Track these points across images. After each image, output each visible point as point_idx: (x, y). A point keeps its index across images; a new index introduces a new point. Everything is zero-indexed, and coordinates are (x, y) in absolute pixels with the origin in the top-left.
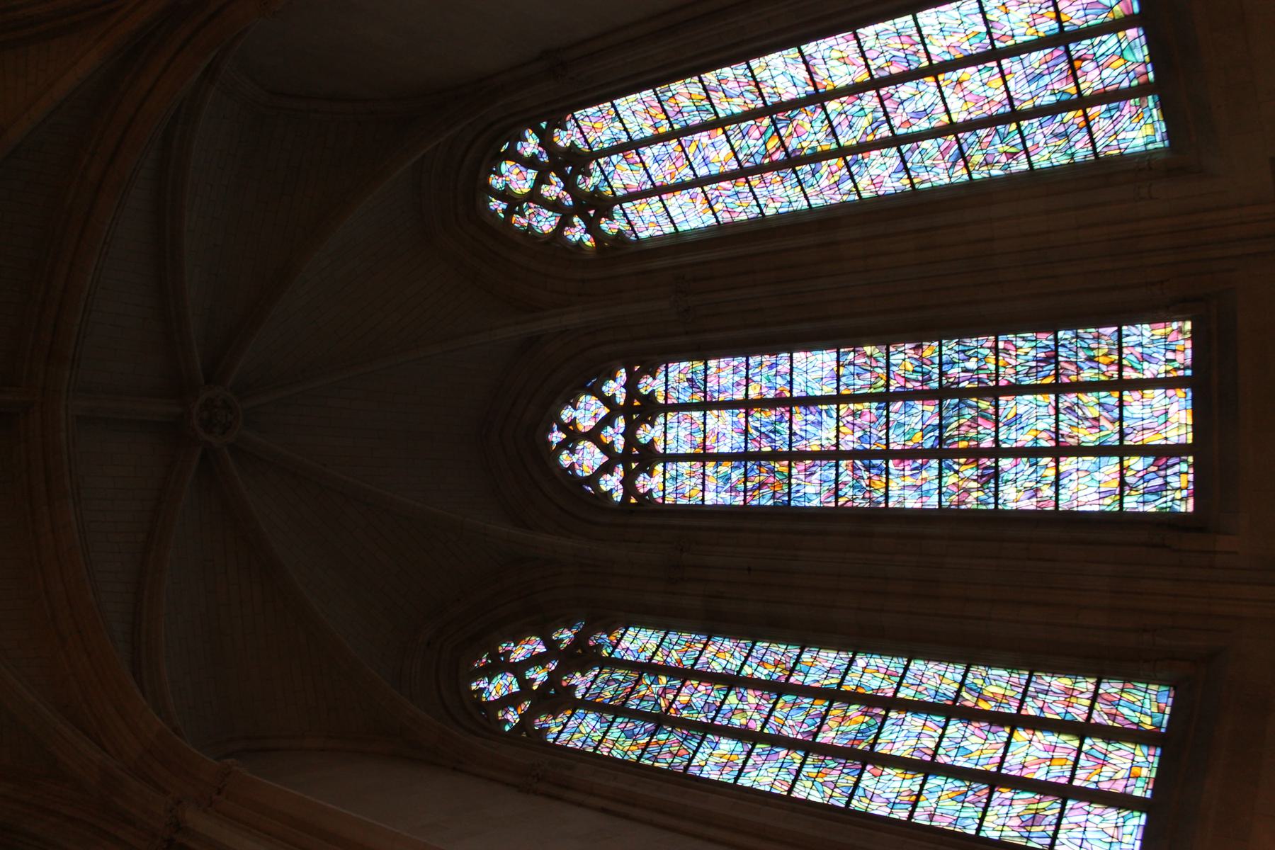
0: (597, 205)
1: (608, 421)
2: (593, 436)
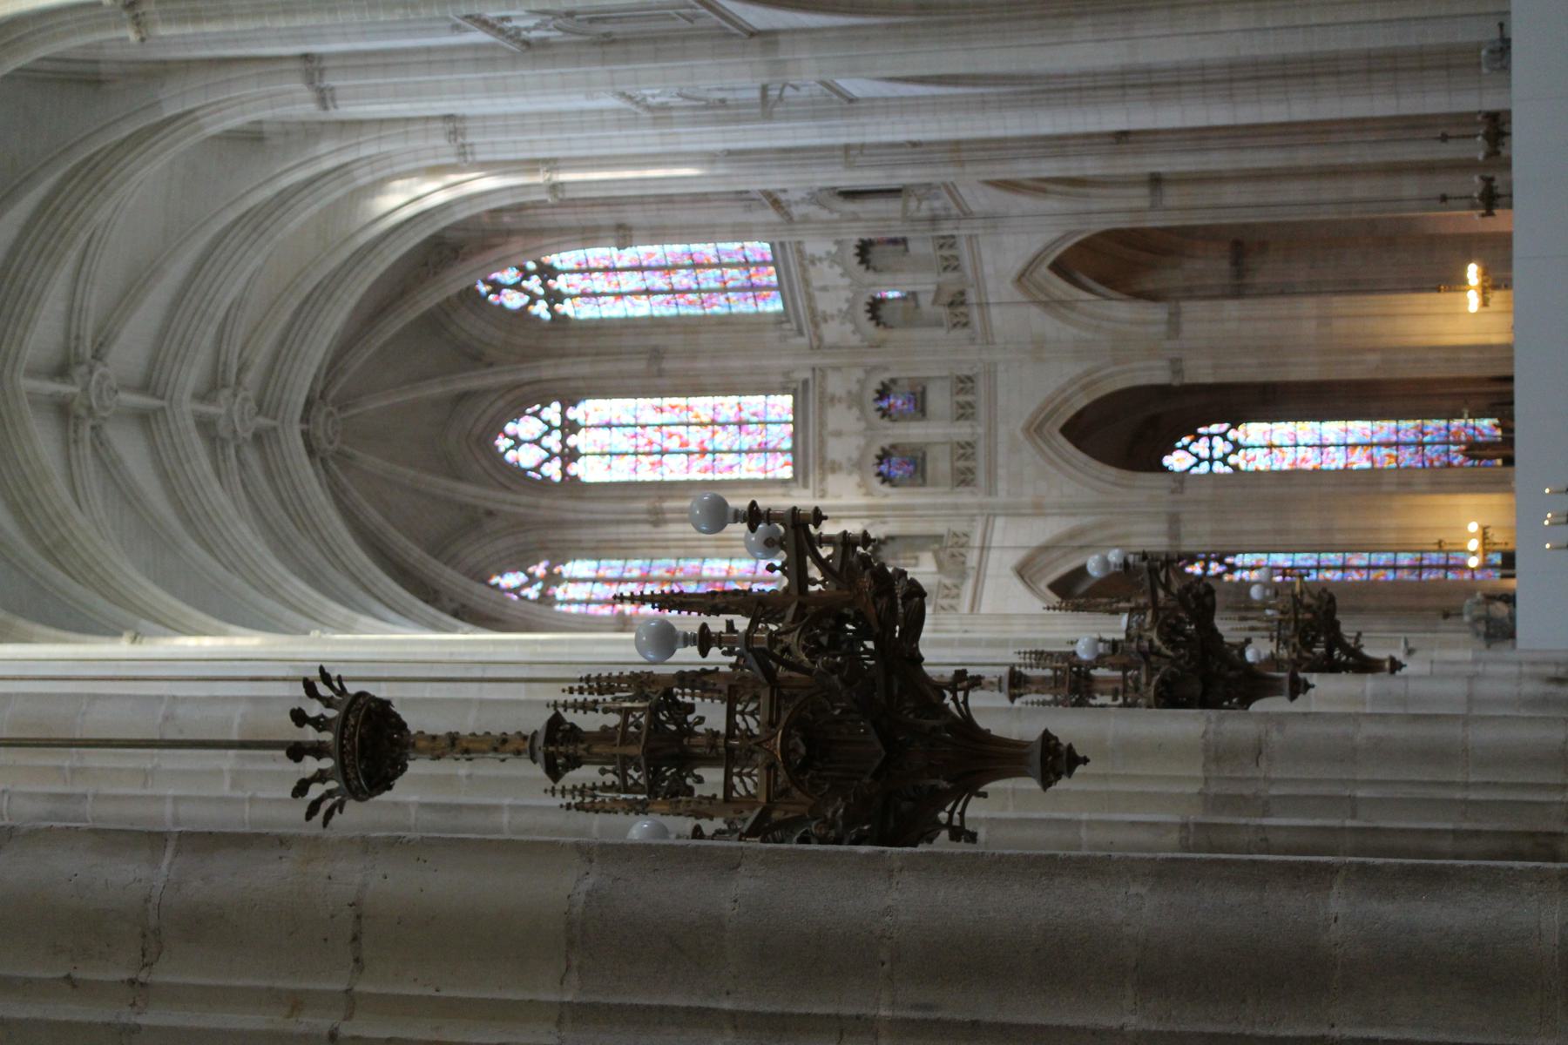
0: (554, 297)
1: (548, 433)
2: (537, 442)
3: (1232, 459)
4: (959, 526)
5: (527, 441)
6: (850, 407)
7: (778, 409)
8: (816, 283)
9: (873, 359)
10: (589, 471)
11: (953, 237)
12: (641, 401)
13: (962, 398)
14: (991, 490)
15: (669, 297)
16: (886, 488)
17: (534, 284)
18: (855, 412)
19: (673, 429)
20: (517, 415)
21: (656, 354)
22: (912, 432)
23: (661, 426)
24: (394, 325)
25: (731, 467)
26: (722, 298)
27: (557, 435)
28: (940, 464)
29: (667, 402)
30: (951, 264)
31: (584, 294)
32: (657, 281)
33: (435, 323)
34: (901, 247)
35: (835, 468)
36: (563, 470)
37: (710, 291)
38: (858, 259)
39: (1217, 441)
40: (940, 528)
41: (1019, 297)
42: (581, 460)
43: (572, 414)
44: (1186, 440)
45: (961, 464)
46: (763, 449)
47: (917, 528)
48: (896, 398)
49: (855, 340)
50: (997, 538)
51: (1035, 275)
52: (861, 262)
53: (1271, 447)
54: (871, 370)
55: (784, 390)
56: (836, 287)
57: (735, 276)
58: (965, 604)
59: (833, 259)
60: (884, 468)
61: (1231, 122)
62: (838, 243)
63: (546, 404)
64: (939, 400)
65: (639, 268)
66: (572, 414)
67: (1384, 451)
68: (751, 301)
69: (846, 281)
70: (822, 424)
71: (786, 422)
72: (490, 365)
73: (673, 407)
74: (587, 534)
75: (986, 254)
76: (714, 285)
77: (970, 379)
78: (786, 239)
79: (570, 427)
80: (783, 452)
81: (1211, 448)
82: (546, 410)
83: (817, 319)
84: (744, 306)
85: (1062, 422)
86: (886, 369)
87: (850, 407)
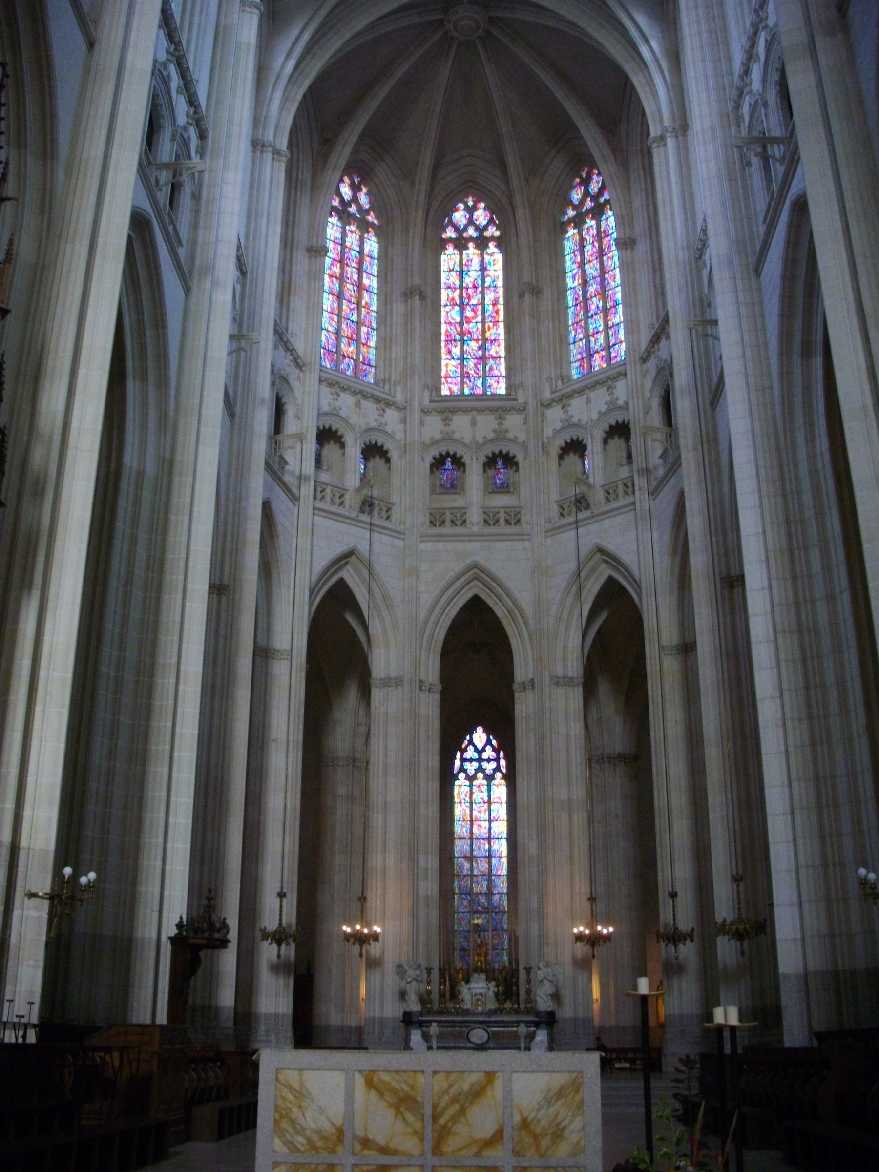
1: (477, 228)
2: (471, 222)
4: (395, 513)
6: (494, 431)
7: (495, 385)
8: (593, 395)
10: (449, 258)
11: (634, 493)
12: (501, 291)
13: (502, 516)
14: (425, 537)
15: (581, 299)
16: (429, 460)
17: (589, 204)
18: (491, 436)
19: (480, 313)
21: (536, 291)
22: (475, 477)
23: (483, 304)
25: (449, 352)
26: (581, 336)
27: (475, 235)
29: (501, 308)
31: (582, 240)
32: (592, 289)
34: (624, 462)
35: (447, 421)
36: (450, 240)
37: (586, 328)
38: (613, 423)
39: (493, 765)
41: (584, 552)
42: (456, 252)
43: (491, 245)
44: (494, 742)
46: (464, 376)
47: (396, 481)
48: (501, 461)
49: (548, 432)
51: (604, 565)
52: (611, 427)
53: (489, 802)
54: (524, 446)
57: (597, 323)
59: (613, 407)
60: (449, 465)
61: (753, 639)
62: (627, 403)
64: (501, 501)
65: (603, 271)
66: (492, 248)
67: (485, 884)
68: (579, 357)
69: (595, 416)
70: (481, 410)
71: (485, 391)
72: (527, 180)
73: (497, 312)
75: (619, 520)
76: (591, 327)
78: (628, 364)
79: (482, 243)
80: (462, 389)
81: (489, 760)
82: (495, 228)
84: (575, 352)
85: (483, 596)
87: (494, 431)
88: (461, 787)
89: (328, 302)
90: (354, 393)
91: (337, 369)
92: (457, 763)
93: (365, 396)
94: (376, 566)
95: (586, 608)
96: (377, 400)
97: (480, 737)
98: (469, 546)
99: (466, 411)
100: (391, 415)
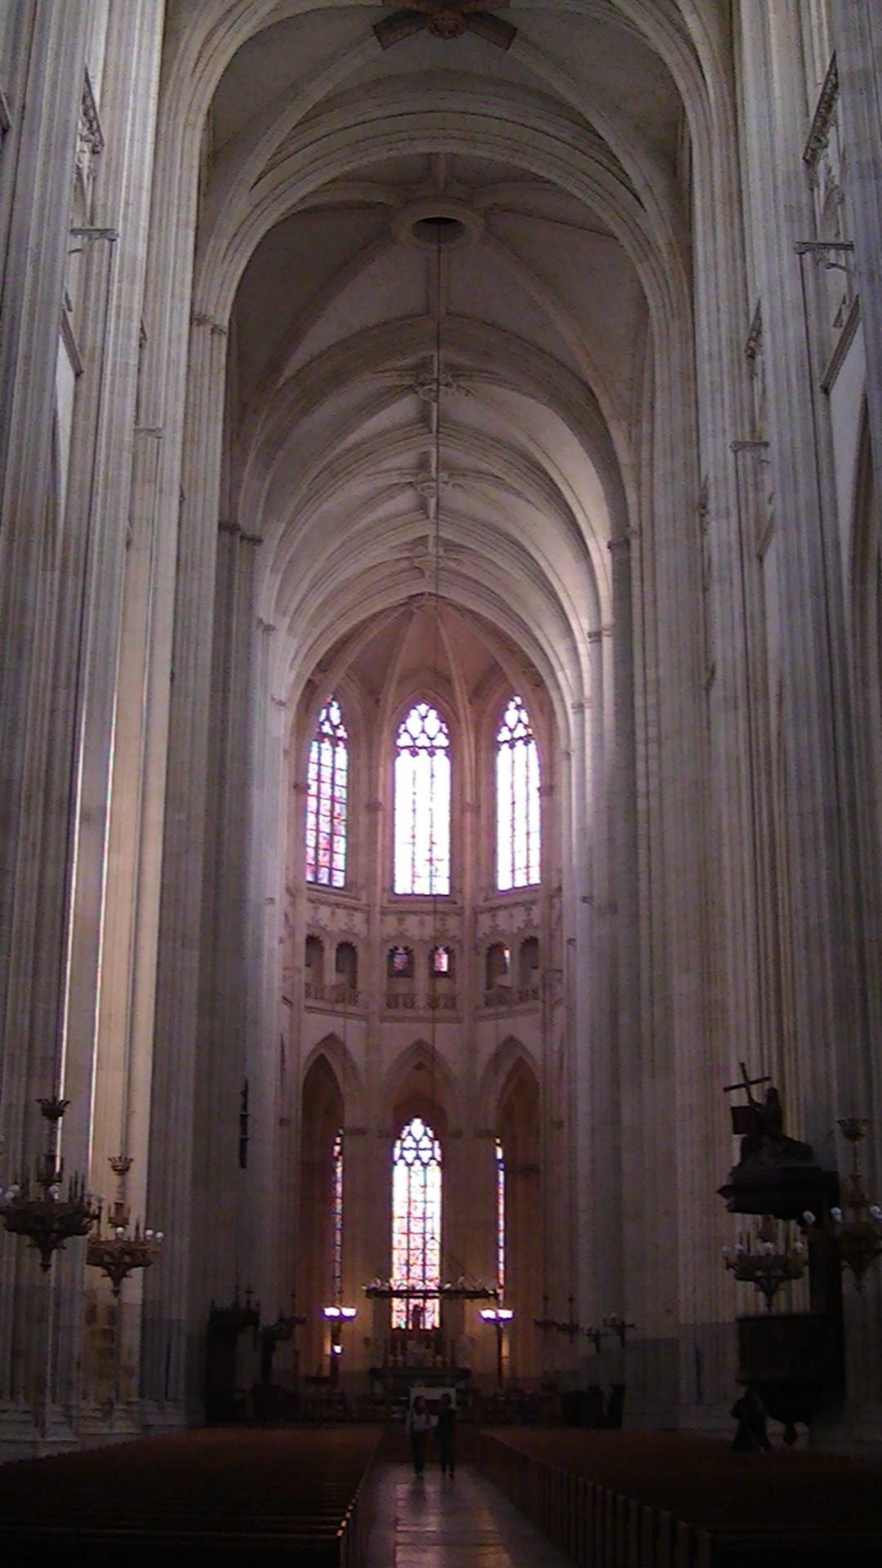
0: (512, 743)
3: (417, 1162)
5: (423, 723)
8: (515, 911)
9: (467, 946)
10: (404, 761)
16: (387, 952)
17: (521, 732)
20: (442, 718)
24: (492, 647)
27: (427, 743)
28: (402, 986)
30: (523, 997)
33: (494, 671)
35: (401, 921)
40: (361, 986)
44: (430, 1133)
45: (401, 1000)
49: (480, 935)
50: (353, 1023)
53: (425, 1186)
55: (452, 888)
56: (511, 923)
58: (311, 1003)
59: (528, 923)
60: (401, 950)
63: (447, 736)
66: (440, 753)
74: (362, 762)
77: (454, 1006)
83: (493, 910)
86: (462, 953)
88: (399, 1172)
89: (311, 820)
90: (329, 904)
91: (315, 882)
92: (397, 1152)
93: (338, 905)
94: (347, 1045)
95: (502, 1078)
96: (346, 907)
97: (417, 1127)
98: (415, 1026)
99: (415, 913)
100: (359, 917)
